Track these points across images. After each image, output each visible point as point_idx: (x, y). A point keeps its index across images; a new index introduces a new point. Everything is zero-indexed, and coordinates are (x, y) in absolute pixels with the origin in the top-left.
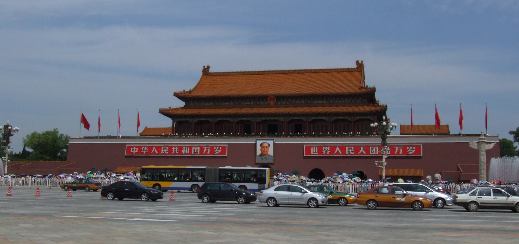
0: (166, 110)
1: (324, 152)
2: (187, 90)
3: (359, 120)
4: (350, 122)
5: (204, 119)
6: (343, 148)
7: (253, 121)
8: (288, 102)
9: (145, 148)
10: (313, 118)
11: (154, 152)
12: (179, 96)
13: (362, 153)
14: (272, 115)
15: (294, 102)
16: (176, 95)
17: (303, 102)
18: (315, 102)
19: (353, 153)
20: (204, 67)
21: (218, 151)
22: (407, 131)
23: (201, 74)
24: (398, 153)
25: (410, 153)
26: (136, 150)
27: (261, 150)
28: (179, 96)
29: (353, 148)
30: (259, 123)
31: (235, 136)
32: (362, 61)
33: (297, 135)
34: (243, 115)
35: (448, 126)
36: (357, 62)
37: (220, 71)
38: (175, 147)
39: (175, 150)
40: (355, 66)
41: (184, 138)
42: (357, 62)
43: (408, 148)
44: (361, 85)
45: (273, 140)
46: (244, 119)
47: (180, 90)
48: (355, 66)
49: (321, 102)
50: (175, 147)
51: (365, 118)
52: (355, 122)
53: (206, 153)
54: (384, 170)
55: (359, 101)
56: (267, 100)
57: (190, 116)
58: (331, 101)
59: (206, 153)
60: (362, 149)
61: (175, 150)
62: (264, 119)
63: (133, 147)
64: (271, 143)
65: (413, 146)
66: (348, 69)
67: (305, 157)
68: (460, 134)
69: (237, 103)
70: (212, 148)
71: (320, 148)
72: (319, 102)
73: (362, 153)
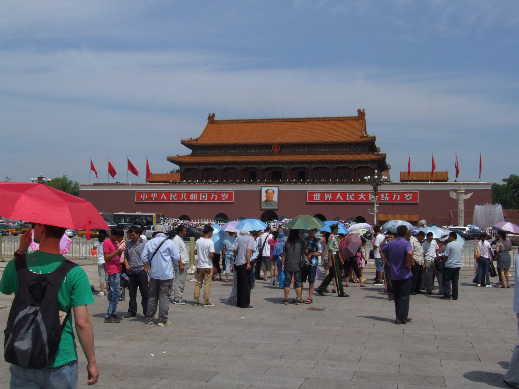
0: (174, 158)
1: (326, 199)
2: (194, 138)
3: (359, 168)
4: (351, 169)
5: (211, 167)
6: (344, 195)
7: (258, 168)
8: (291, 150)
9: (155, 195)
10: (316, 166)
11: (163, 199)
12: (186, 144)
13: (362, 199)
14: (277, 163)
15: (297, 150)
16: (185, 143)
17: (306, 150)
18: (318, 150)
19: (353, 199)
20: (210, 115)
21: (225, 197)
22: (408, 178)
23: (206, 122)
24: (396, 200)
25: (407, 199)
26: (145, 196)
27: (266, 196)
28: (186, 144)
29: (353, 194)
30: (264, 170)
31: (241, 183)
32: (363, 110)
33: (301, 182)
34: (248, 163)
35: (447, 173)
36: (359, 111)
37: (225, 119)
38: (184, 193)
39: (184, 196)
40: (356, 114)
41: (192, 185)
42: (359, 111)
43: (405, 195)
44: (362, 134)
45: (278, 187)
46: (249, 166)
47: (187, 138)
48: (356, 114)
49: (324, 150)
50: (184, 193)
51: (365, 165)
52: (356, 169)
53: (214, 199)
54: (376, 217)
55: (359, 150)
56: (271, 148)
57: (198, 164)
58: (333, 150)
59: (214, 199)
60: (362, 196)
61: (184, 196)
62: (268, 166)
63: (142, 193)
64: (276, 189)
65: (410, 193)
66: (350, 117)
67: (308, 203)
68: (455, 181)
69: (243, 151)
70: (219, 195)
71: (322, 195)
72: (321, 150)
73: (362, 199)
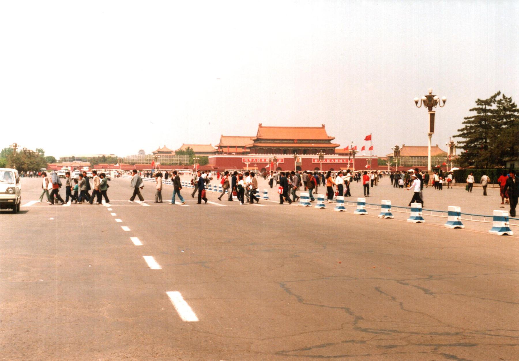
39: (263, 160)
40: (321, 126)
61: (263, 160)
